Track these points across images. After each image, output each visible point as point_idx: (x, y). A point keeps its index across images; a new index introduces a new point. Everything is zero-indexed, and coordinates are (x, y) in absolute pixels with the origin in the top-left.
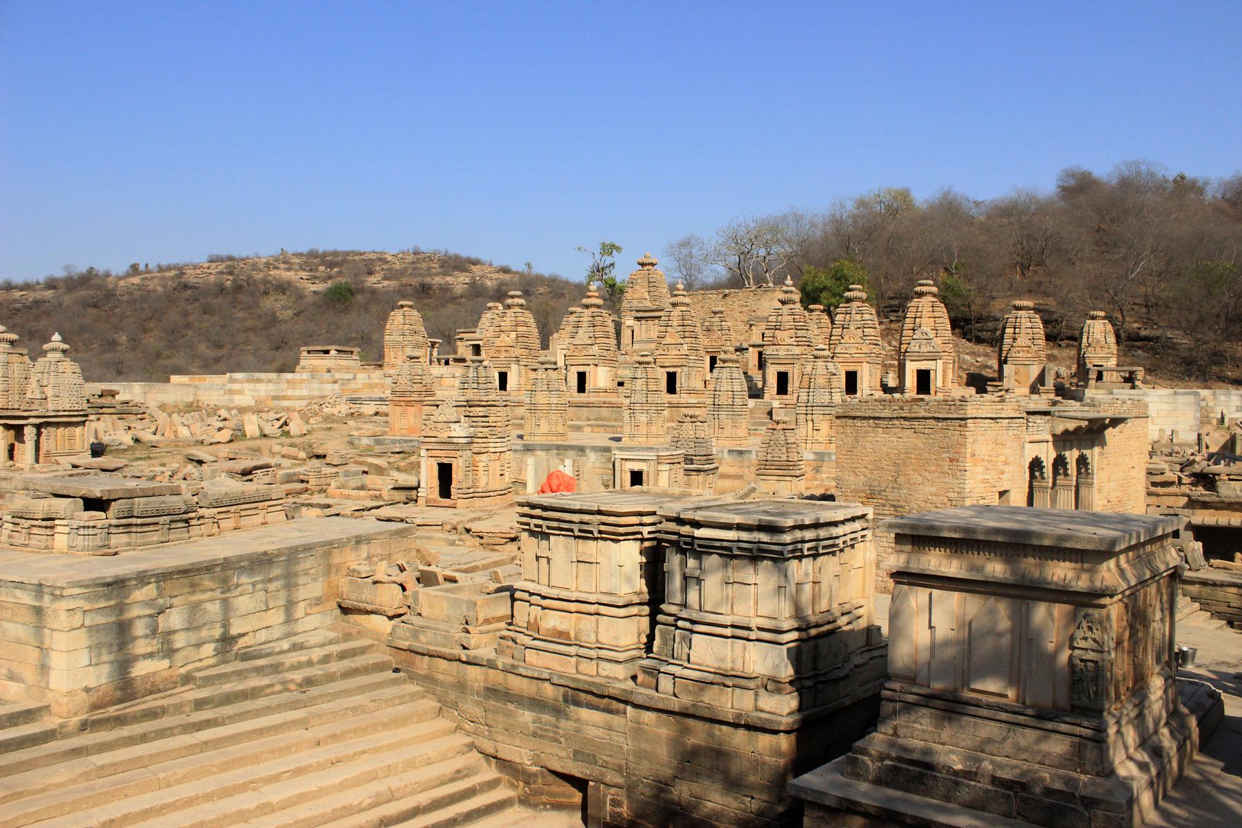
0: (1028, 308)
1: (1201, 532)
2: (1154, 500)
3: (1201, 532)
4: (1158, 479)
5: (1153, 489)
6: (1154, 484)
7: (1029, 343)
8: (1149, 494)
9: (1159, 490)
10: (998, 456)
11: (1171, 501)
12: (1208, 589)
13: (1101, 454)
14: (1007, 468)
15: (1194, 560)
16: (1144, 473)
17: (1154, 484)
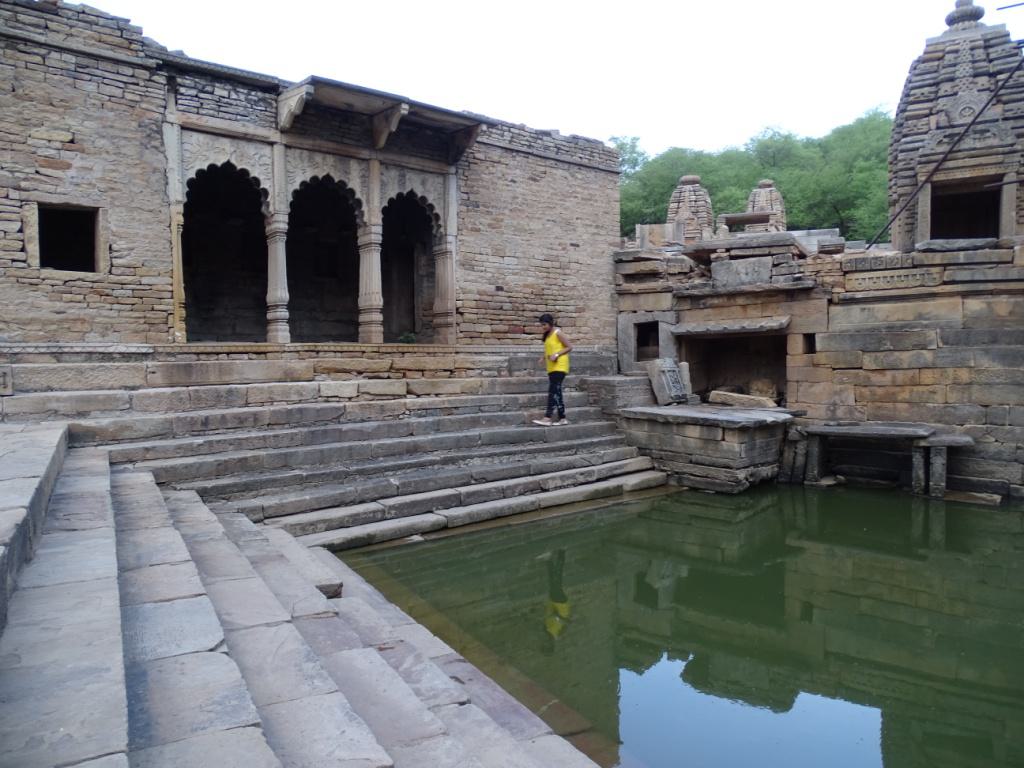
0: (693, 182)
1: (689, 345)
2: (627, 303)
3: (689, 345)
4: (631, 268)
5: (626, 286)
6: (629, 278)
7: (692, 216)
8: (622, 293)
9: (635, 287)
10: (26, 123)
11: (647, 302)
12: (659, 431)
13: (470, 204)
14: (77, 161)
15: (662, 387)
16: (611, 260)
17: (629, 278)
